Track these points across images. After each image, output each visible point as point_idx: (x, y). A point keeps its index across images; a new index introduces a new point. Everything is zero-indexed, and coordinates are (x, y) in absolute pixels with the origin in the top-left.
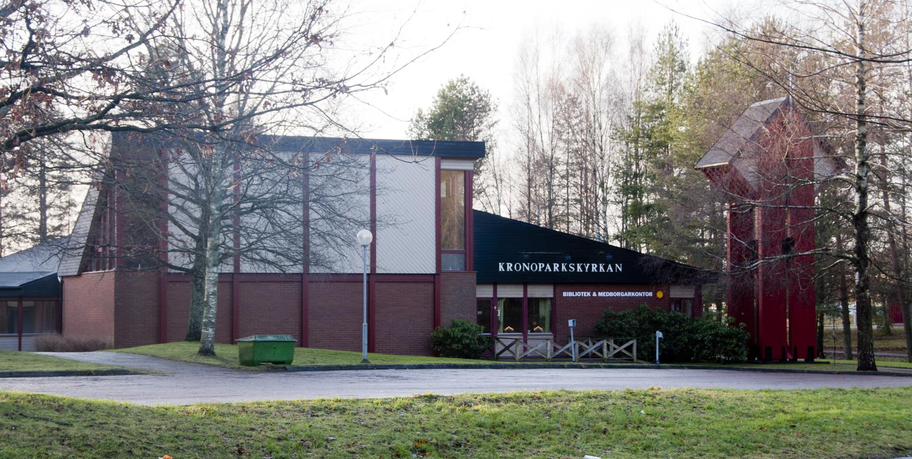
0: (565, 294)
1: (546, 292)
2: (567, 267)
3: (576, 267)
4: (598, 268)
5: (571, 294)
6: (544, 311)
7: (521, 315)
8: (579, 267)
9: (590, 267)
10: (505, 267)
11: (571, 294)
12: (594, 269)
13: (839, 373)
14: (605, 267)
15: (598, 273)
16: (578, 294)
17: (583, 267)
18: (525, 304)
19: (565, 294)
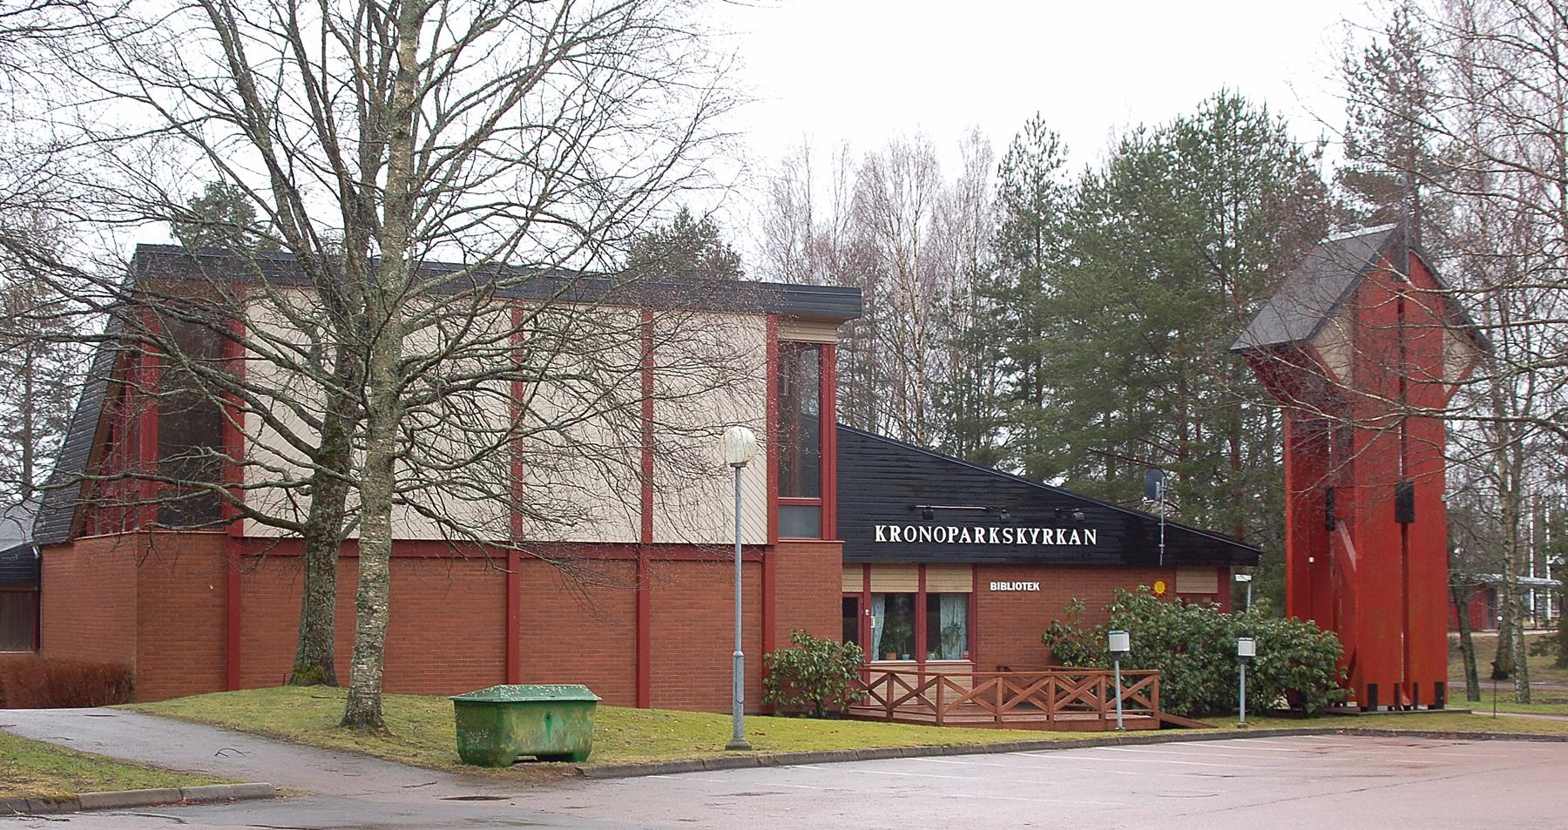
0: (993, 586)
1: (961, 583)
2: (999, 534)
3: (1015, 535)
4: (1054, 538)
5: (1004, 586)
6: (950, 617)
7: (914, 624)
8: (1020, 535)
9: (1041, 534)
10: (887, 532)
11: (1004, 586)
12: (1047, 539)
13: (1460, 736)
14: (1067, 536)
15: (1055, 546)
16: (1017, 586)
17: (1027, 535)
18: (922, 604)
19: (993, 586)
